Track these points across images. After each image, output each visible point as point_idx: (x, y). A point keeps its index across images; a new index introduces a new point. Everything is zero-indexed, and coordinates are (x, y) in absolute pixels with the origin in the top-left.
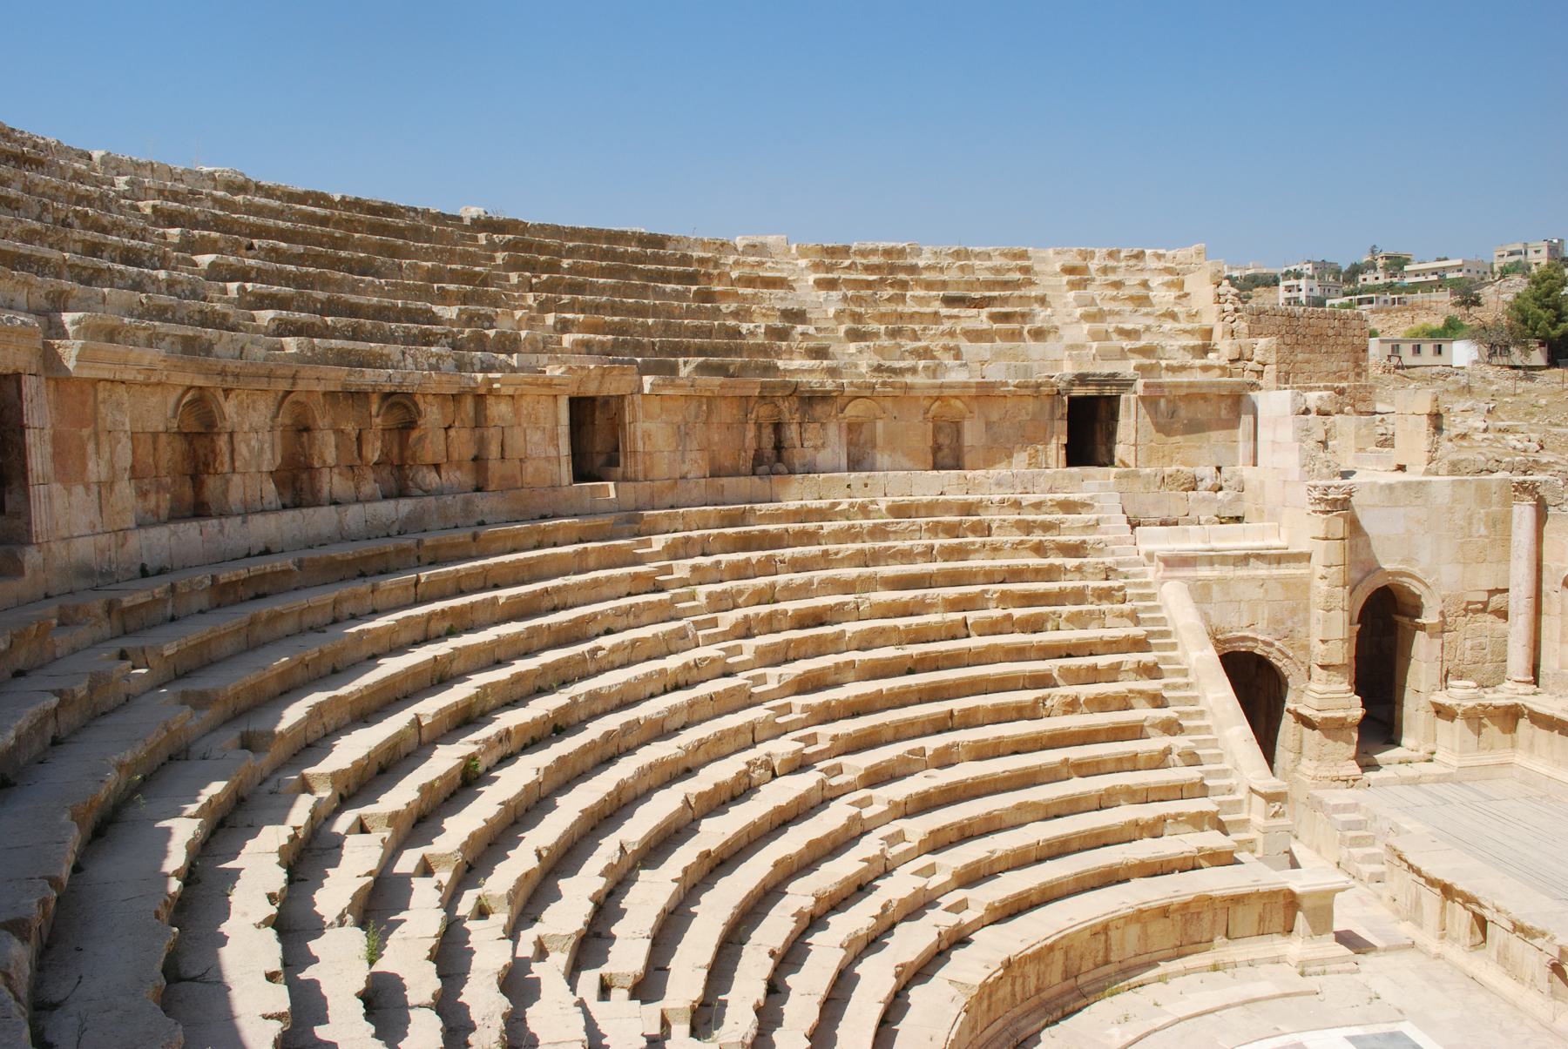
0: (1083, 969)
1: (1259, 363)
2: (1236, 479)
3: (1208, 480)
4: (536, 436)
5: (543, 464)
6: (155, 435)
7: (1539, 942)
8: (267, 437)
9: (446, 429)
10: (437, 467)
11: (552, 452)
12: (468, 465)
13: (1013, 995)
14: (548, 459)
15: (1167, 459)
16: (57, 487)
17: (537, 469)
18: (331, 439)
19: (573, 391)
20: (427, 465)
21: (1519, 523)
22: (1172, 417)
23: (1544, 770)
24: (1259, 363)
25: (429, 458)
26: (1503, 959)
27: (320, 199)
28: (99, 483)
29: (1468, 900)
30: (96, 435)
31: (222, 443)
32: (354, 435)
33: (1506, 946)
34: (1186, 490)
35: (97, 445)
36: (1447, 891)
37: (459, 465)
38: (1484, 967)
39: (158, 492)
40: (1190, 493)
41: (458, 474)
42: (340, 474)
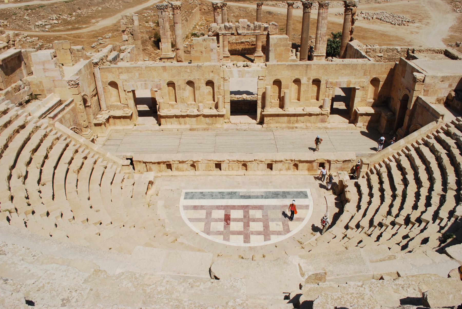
1: (13, 41)
2: (27, 82)
3: (22, 85)
7: (187, 163)
15: (10, 83)
21: (97, 73)
22: (7, 68)
23: (121, 128)
24: (13, 41)
26: (177, 169)
29: (164, 163)
33: (178, 167)
34: (19, 91)
36: (159, 163)
38: (174, 172)
40: (20, 91)
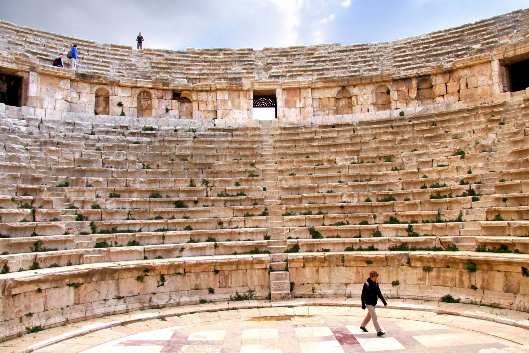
0: (521, 292)
4: (483, 78)
5: (486, 87)
6: (329, 98)
8: (370, 95)
9: (446, 84)
10: (443, 96)
11: (490, 82)
12: (456, 93)
13: (461, 281)
14: (489, 85)
16: (286, 109)
17: (483, 90)
18: (396, 93)
19: (501, 57)
20: (439, 96)
25: (438, 94)
27: (470, 25)
28: (300, 108)
30: (300, 99)
31: (353, 98)
32: (406, 91)
35: (300, 101)
37: (452, 94)
39: (329, 110)
41: (452, 97)
42: (400, 102)
